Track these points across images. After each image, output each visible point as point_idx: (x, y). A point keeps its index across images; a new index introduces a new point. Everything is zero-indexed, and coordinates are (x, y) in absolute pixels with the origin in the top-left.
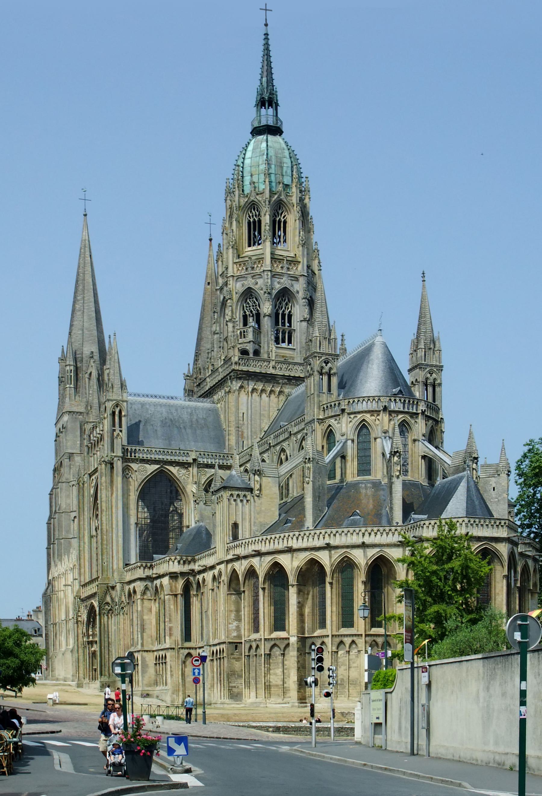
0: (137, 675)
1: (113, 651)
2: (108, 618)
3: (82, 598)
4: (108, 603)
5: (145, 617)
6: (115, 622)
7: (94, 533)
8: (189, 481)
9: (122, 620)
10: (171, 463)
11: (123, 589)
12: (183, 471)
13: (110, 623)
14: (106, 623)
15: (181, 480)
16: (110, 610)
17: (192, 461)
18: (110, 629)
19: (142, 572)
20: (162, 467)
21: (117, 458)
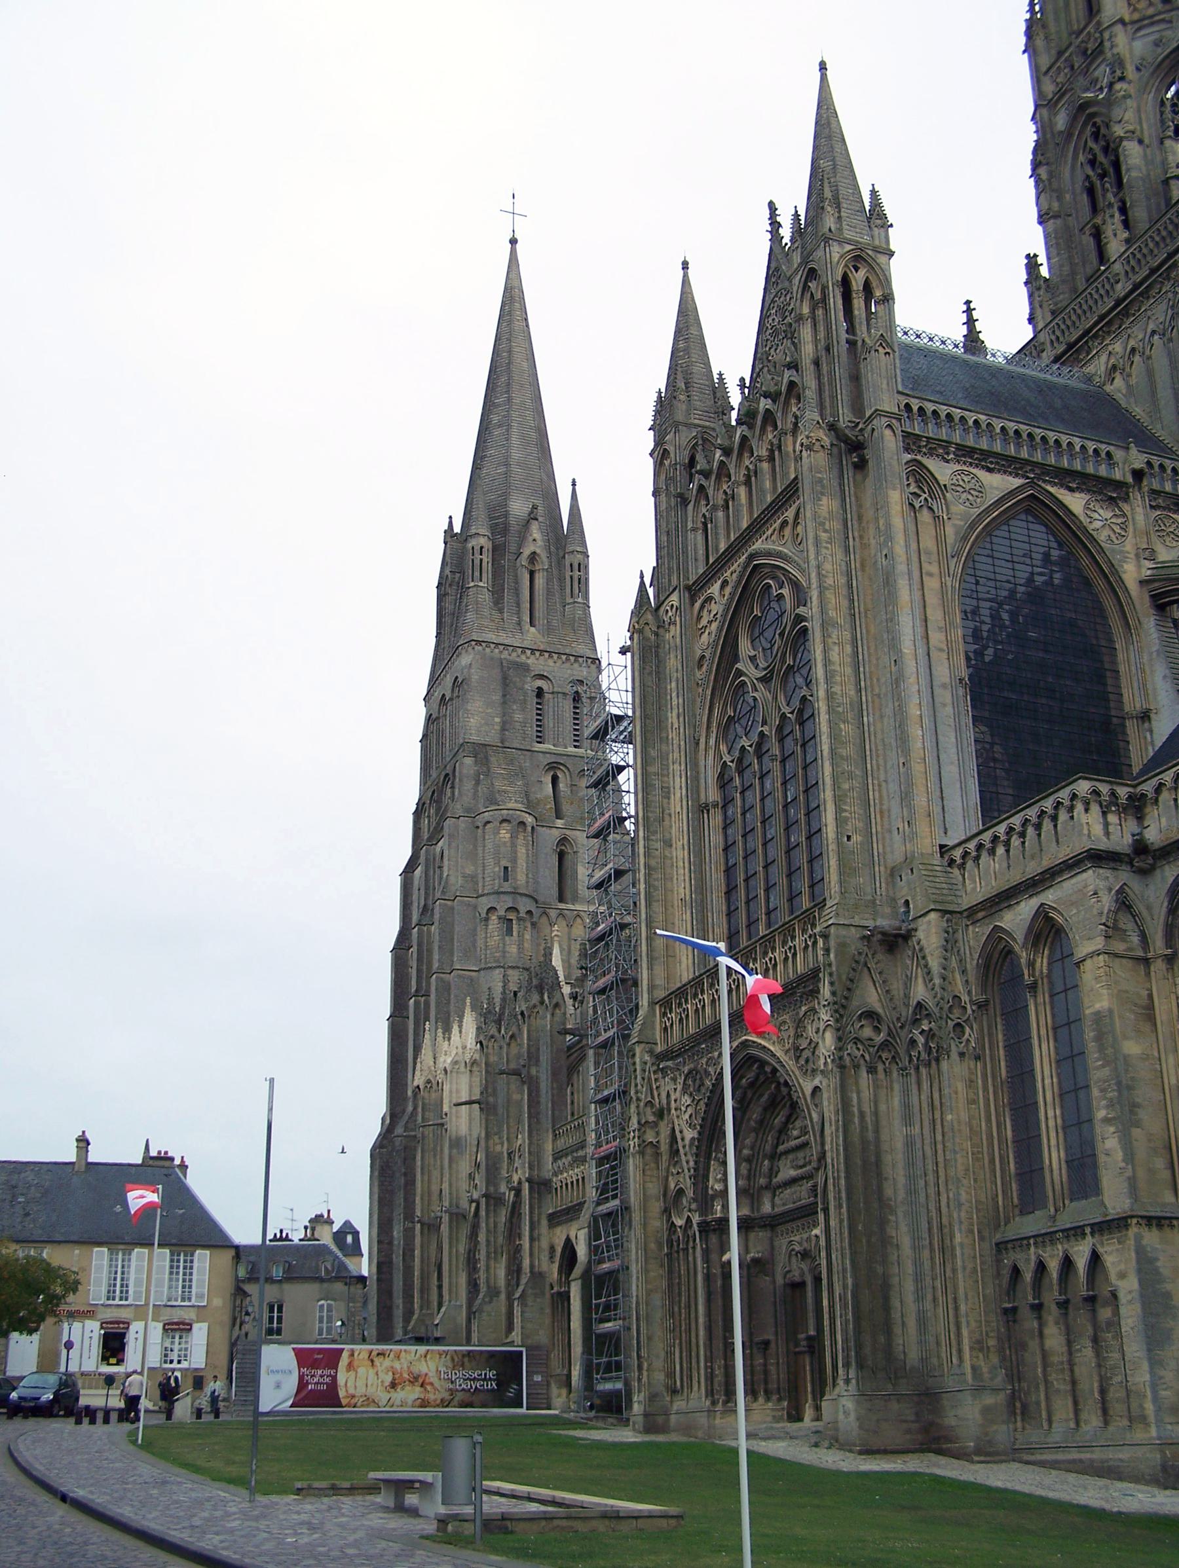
0: (1086, 1353)
1: (906, 1242)
2: (877, 1087)
3: (659, 1049)
4: (870, 1015)
5: (1132, 1048)
6: (906, 1106)
7: (712, 794)
8: (1129, 546)
9: (960, 1086)
10: (1066, 477)
11: (950, 944)
12: (1101, 511)
13: (883, 1107)
14: (866, 1109)
15: (1102, 537)
16: (885, 1045)
17: (1130, 479)
18: (884, 1136)
19: (1098, 829)
20: (1032, 484)
21: (884, 420)
